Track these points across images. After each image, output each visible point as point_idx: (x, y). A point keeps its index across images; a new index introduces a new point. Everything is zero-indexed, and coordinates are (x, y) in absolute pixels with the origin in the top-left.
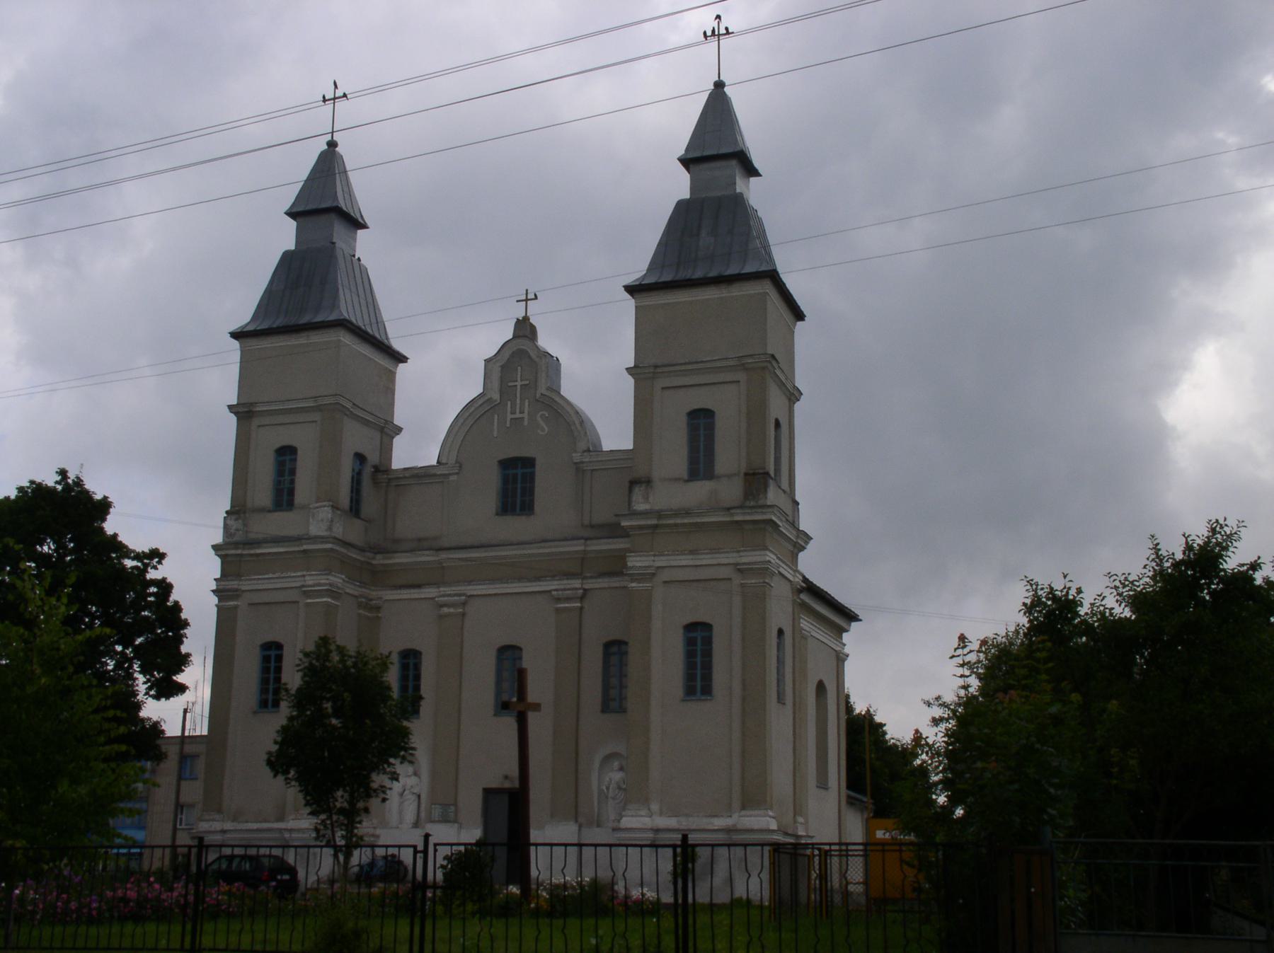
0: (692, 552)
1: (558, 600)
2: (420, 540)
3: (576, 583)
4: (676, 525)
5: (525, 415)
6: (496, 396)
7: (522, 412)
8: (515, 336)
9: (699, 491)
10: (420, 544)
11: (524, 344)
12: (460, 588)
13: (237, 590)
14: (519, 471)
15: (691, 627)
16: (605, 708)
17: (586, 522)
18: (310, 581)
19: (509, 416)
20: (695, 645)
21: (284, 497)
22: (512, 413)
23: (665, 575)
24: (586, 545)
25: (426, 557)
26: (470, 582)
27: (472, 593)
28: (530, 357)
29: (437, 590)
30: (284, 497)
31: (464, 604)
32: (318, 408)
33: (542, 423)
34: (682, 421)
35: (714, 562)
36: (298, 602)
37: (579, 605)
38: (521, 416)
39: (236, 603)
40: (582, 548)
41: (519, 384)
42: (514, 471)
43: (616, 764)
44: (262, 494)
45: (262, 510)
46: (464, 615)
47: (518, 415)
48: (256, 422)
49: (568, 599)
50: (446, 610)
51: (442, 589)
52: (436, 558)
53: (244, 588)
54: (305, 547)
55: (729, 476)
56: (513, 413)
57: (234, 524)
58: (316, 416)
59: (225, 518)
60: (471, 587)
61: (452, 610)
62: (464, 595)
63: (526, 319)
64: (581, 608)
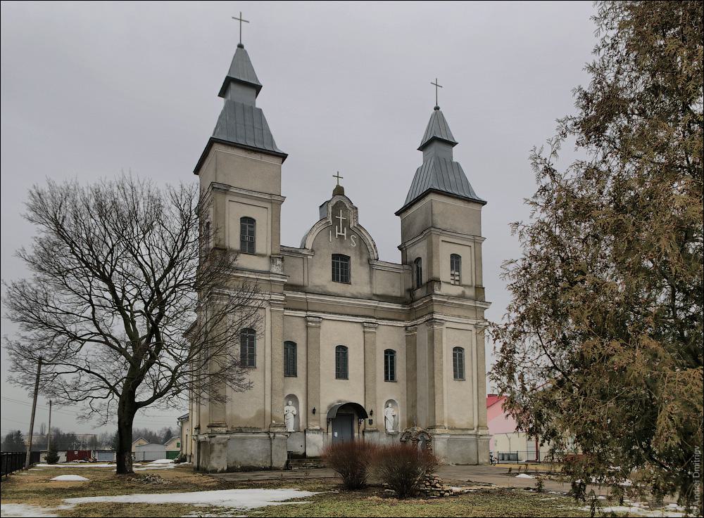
0: (459, 316)
3: (374, 321)
4: (452, 303)
5: (345, 234)
6: (331, 221)
9: (456, 290)
11: (338, 198)
15: (455, 349)
16: (386, 379)
17: (374, 293)
18: (274, 297)
19: (337, 233)
23: (448, 324)
25: (300, 295)
26: (324, 312)
27: (324, 317)
34: (449, 259)
35: (466, 322)
38: (343, 234)
40: (376, 305)
43: (390, 405)
47: (341, 234)
52: (305, 297)
54: (271, 278)
55: (470, 286)
56: (339, 232)
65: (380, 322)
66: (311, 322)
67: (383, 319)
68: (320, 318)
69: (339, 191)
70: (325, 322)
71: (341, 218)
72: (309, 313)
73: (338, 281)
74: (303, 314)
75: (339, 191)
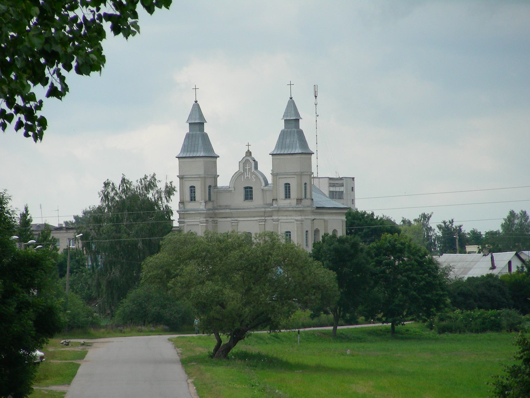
1: (259, 222)
2: (226, 206)
3: (263, 218)
5: (249, 176)
6: (242, 171)
7: (249, 175)
8: (246, 156)
10: (227, 207)
11: (248, 158)
12: (236, 219)
13: (184, 222)
14: (249, 190)
19: (246, 176)
20: (288, 189)
21: (193, 199)
22: (246, 175)
24: (265, 209)
25: (228, 211)
26: (239, 217)
27: (239, 220)
28: (250, 161)
29: (230, 219)
30: (193, 199)
31: (237, 223)
32: (199, 177)
33: (253, 178)
36: (199, 225)
37: (264, 223)
39: (183, 225)
41: (247, 168)
42: (248, 190)
44: (187, 197)
45: (188, 202)
46: (238, 225)
48: (184, 180)
49: (261, 222)
50: (233, 224)
51: (232, 219)
53: (185, 221)
56: (246, 175)
57: (182, 206)
58: (199, 179)
59: (179, 204)
60: (239, 218)
61: (235, 224)
62: (237, 220)
63: (248, 150)
64: (265, 224)
65: (266, 218)
66: (233, 223)
67: (268, 216)
68: (236, 220)
69: (249, 153)
70: (240, 222)
71: (247, 168)
72: (232, 219)
73: (248, 199)
74: (229, 219)
75: (249, 153)
